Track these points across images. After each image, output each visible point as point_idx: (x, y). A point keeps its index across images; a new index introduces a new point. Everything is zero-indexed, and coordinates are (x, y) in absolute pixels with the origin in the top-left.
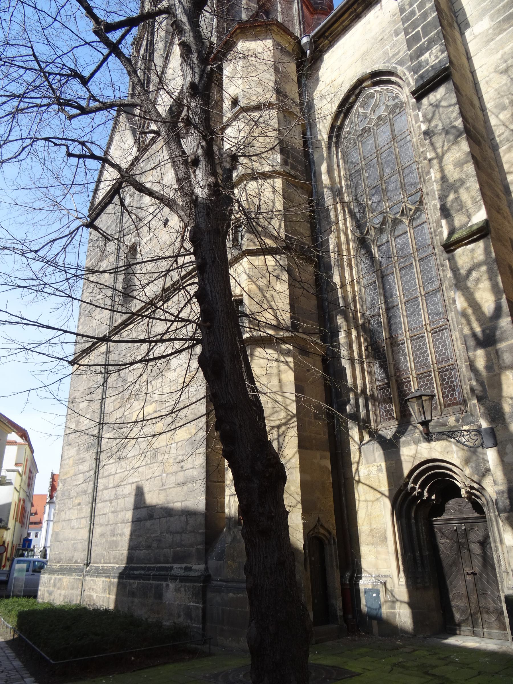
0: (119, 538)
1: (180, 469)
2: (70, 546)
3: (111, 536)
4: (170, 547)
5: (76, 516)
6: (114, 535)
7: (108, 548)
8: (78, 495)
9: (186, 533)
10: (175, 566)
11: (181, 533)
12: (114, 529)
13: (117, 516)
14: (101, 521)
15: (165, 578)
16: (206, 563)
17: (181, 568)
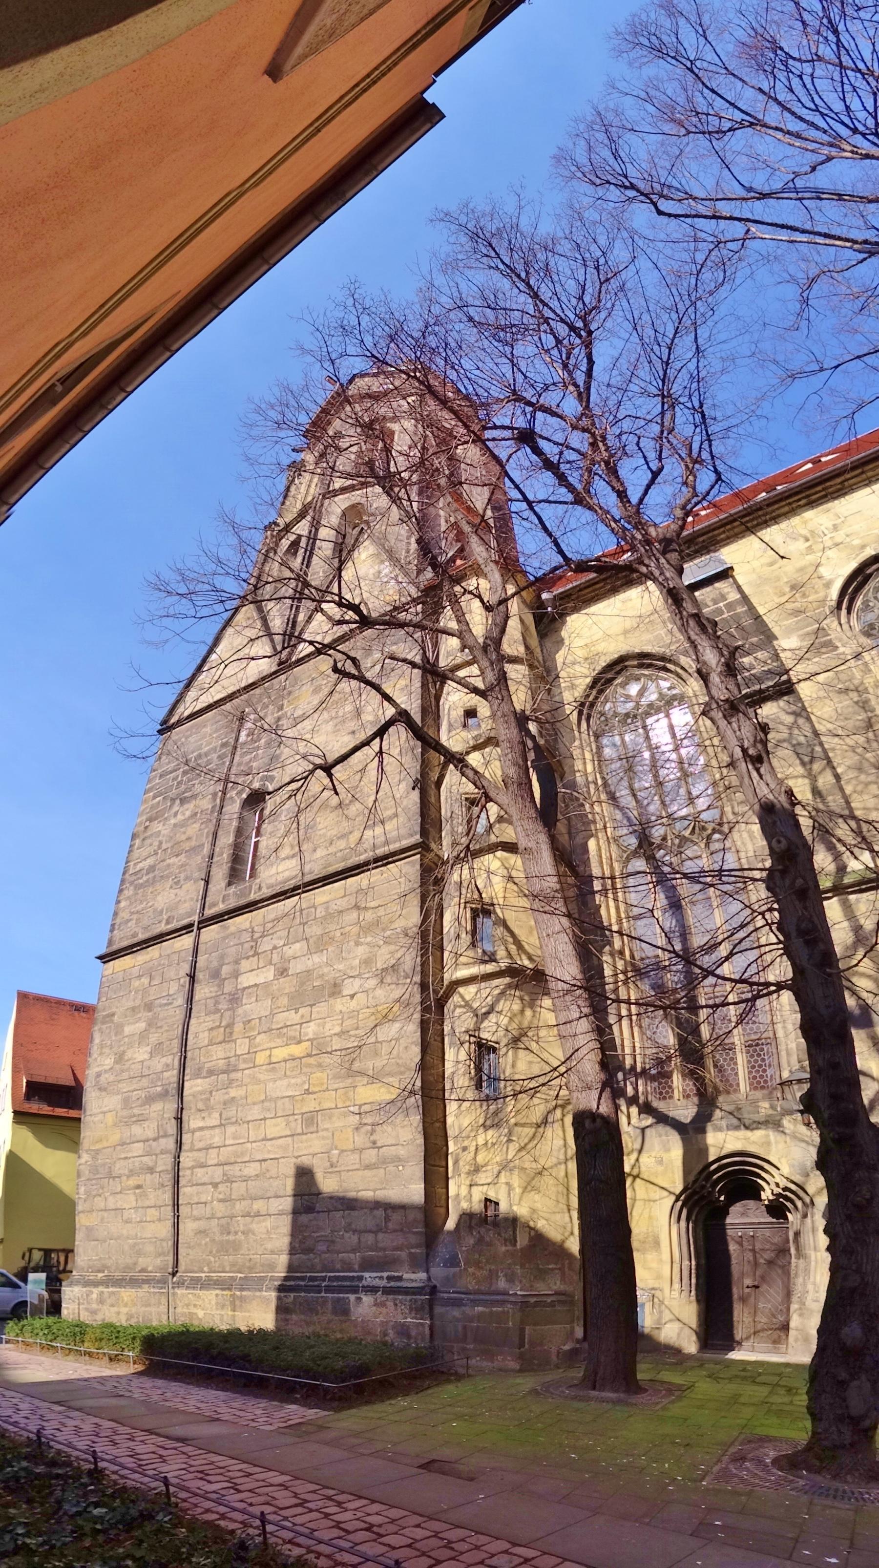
0: (241, 1237)
1: (369, 1145)
2: (126, 1248)
3: (222, 1234)
4: (354, 1251)
5: (134, 1204)
7: (218, 1251)
8: (132, 1173)
9: (385, 1232)
10: (366, 1275)
11: (375, 1233)
12: (228, 1224)
13: (234, 1206)
14: (195, 1213)
15: (354, 1290)
16: (427, 1271)
17: (381, 1278)
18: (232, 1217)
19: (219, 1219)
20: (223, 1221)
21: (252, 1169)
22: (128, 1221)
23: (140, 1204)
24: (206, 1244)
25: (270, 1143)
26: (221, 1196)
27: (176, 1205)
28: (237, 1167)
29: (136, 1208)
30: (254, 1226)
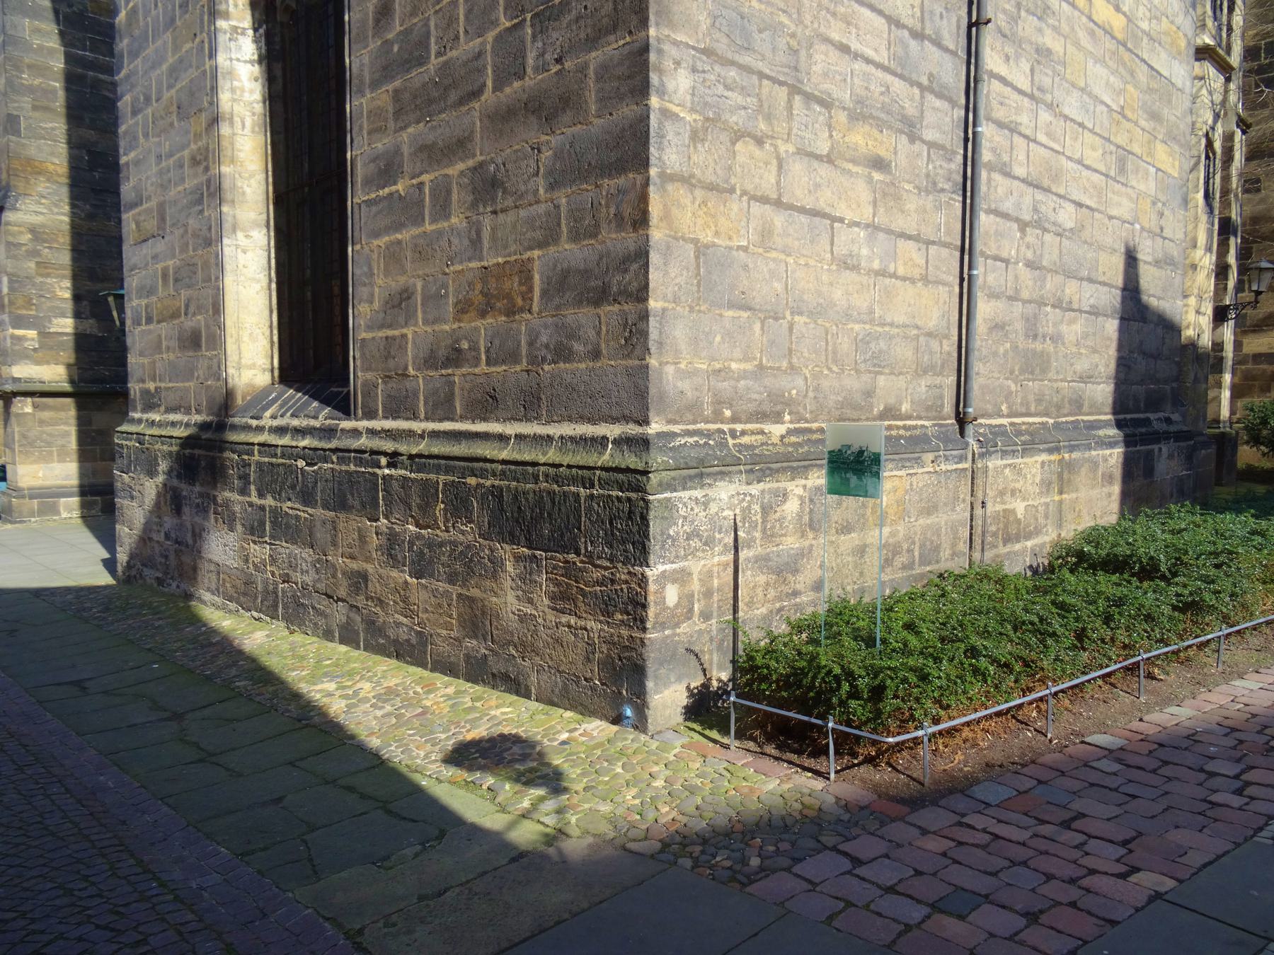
3: (1027, 336)
5: (866, 214)
6: (1035, 337)
18: (1041, 303)
19: (1025, 302)
20: (1031, 309)
21: (1067, 216)
22: (848, 264)
23: (881, 219)
24: (1006, 351)
25: (1086, 173)
26: (1029, 255)
27: (966, 250)
28: (1051, 201)
29: (873, 227)
30: (1064, 328)
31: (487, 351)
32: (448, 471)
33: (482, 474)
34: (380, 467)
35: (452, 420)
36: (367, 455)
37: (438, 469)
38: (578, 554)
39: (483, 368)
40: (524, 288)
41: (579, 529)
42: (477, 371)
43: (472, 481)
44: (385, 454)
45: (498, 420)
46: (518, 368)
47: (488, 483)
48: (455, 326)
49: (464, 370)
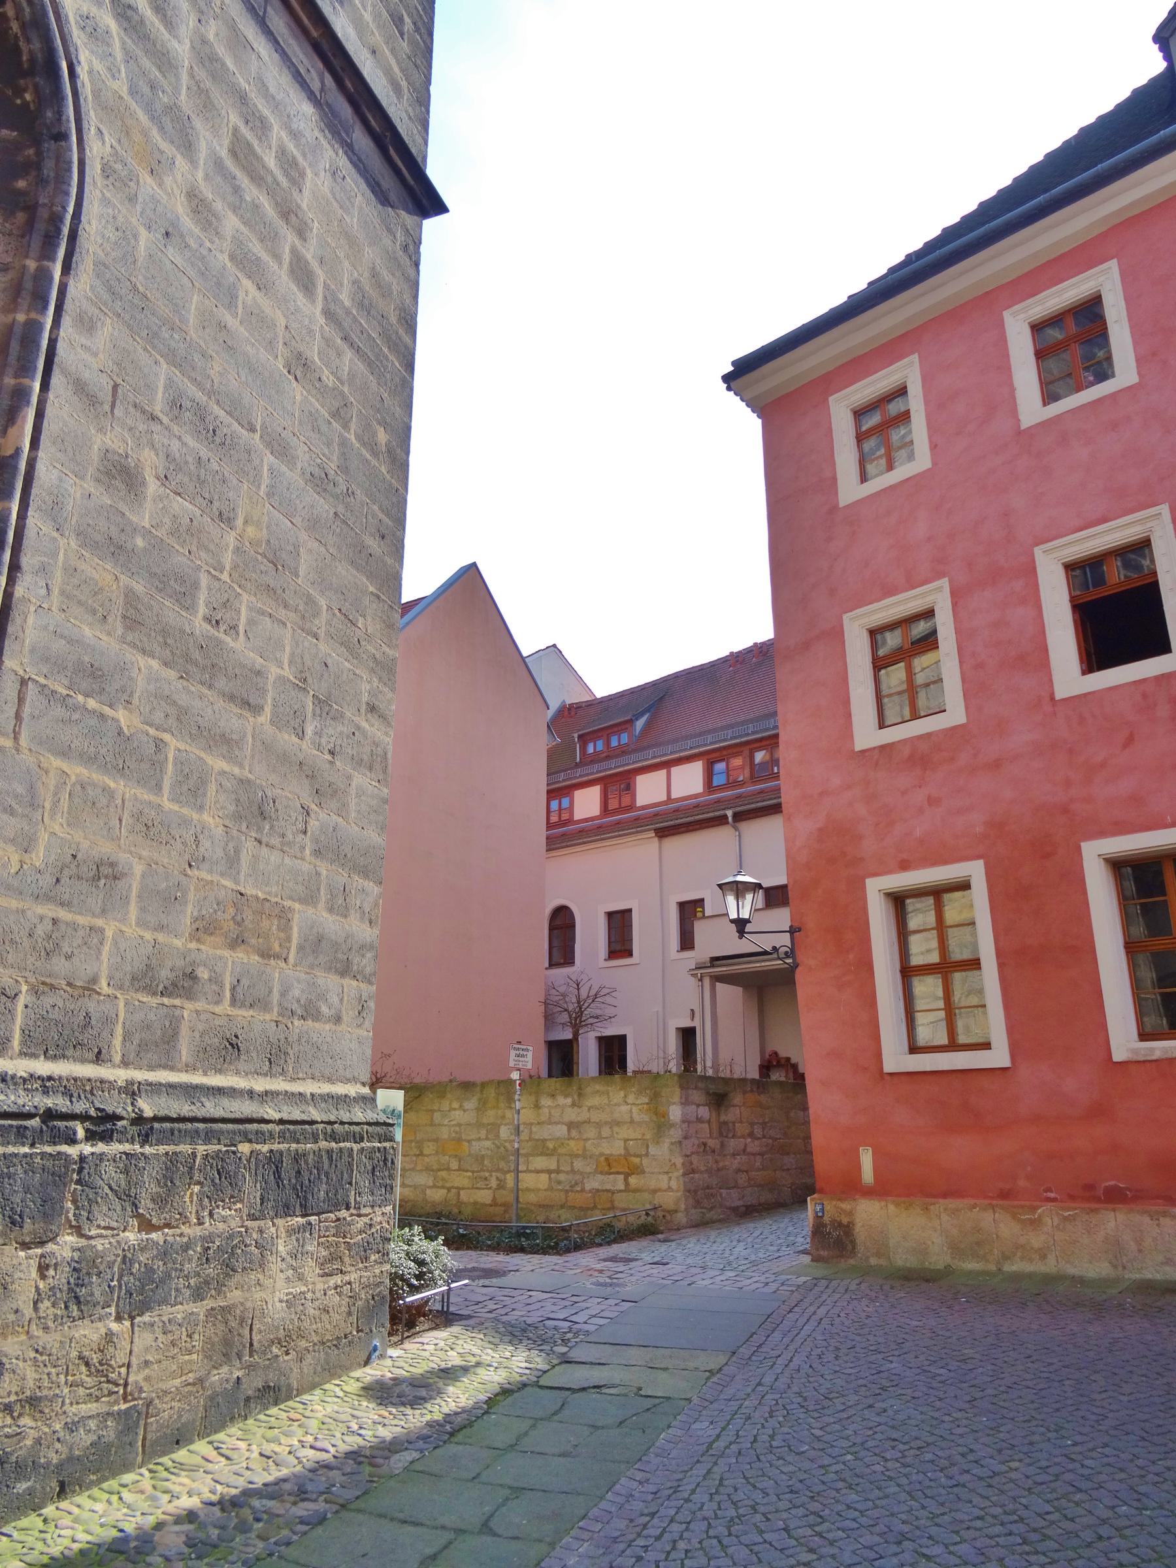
31: (233, 989)
32: (208, 1137)
33: (261, 1137)
34: (72, 1141)
35: (172, 1069)
36: (35, 1122)
37: (194, 1136)
38: (348, 1208)
39: (225, 1007)
40: (282, 935)
41: (350, 1184)
42: (218, 1009)
43: (245, 1148)
44: (83, 1117)
45: (238, 1073)
46: (268, 1017)
47: (265, 1148)
48: (193, 945)
49: (200, 1005)
